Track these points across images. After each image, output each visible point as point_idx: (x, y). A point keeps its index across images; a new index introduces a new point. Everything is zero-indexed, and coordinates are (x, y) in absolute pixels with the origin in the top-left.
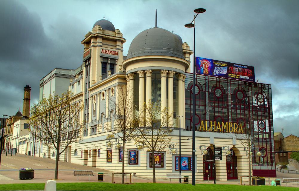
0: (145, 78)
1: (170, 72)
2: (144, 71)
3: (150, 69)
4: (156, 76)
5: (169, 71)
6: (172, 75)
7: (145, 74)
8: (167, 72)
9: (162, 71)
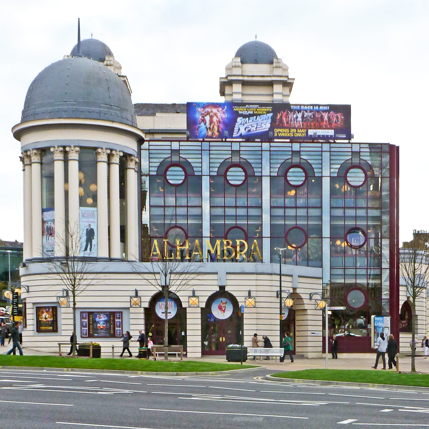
0: (66, 161)
1: (114, 152)
2: (64, 147)
3: (76, 145)
4: (88, 157)
5: (111, 150)
6: (116, 160)
7: (66, 153)
8: (109, 152)
9: (99, 150)
